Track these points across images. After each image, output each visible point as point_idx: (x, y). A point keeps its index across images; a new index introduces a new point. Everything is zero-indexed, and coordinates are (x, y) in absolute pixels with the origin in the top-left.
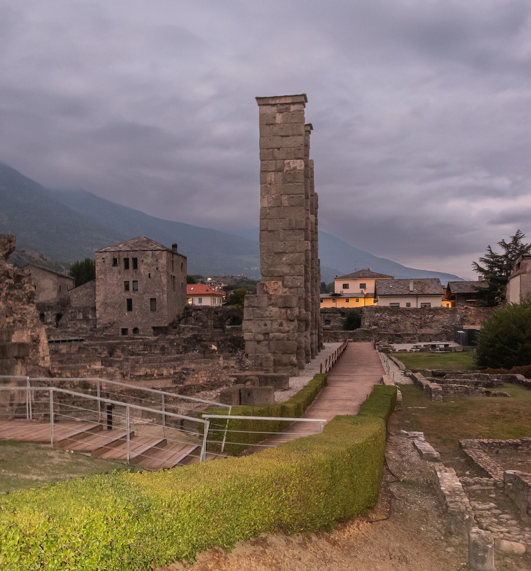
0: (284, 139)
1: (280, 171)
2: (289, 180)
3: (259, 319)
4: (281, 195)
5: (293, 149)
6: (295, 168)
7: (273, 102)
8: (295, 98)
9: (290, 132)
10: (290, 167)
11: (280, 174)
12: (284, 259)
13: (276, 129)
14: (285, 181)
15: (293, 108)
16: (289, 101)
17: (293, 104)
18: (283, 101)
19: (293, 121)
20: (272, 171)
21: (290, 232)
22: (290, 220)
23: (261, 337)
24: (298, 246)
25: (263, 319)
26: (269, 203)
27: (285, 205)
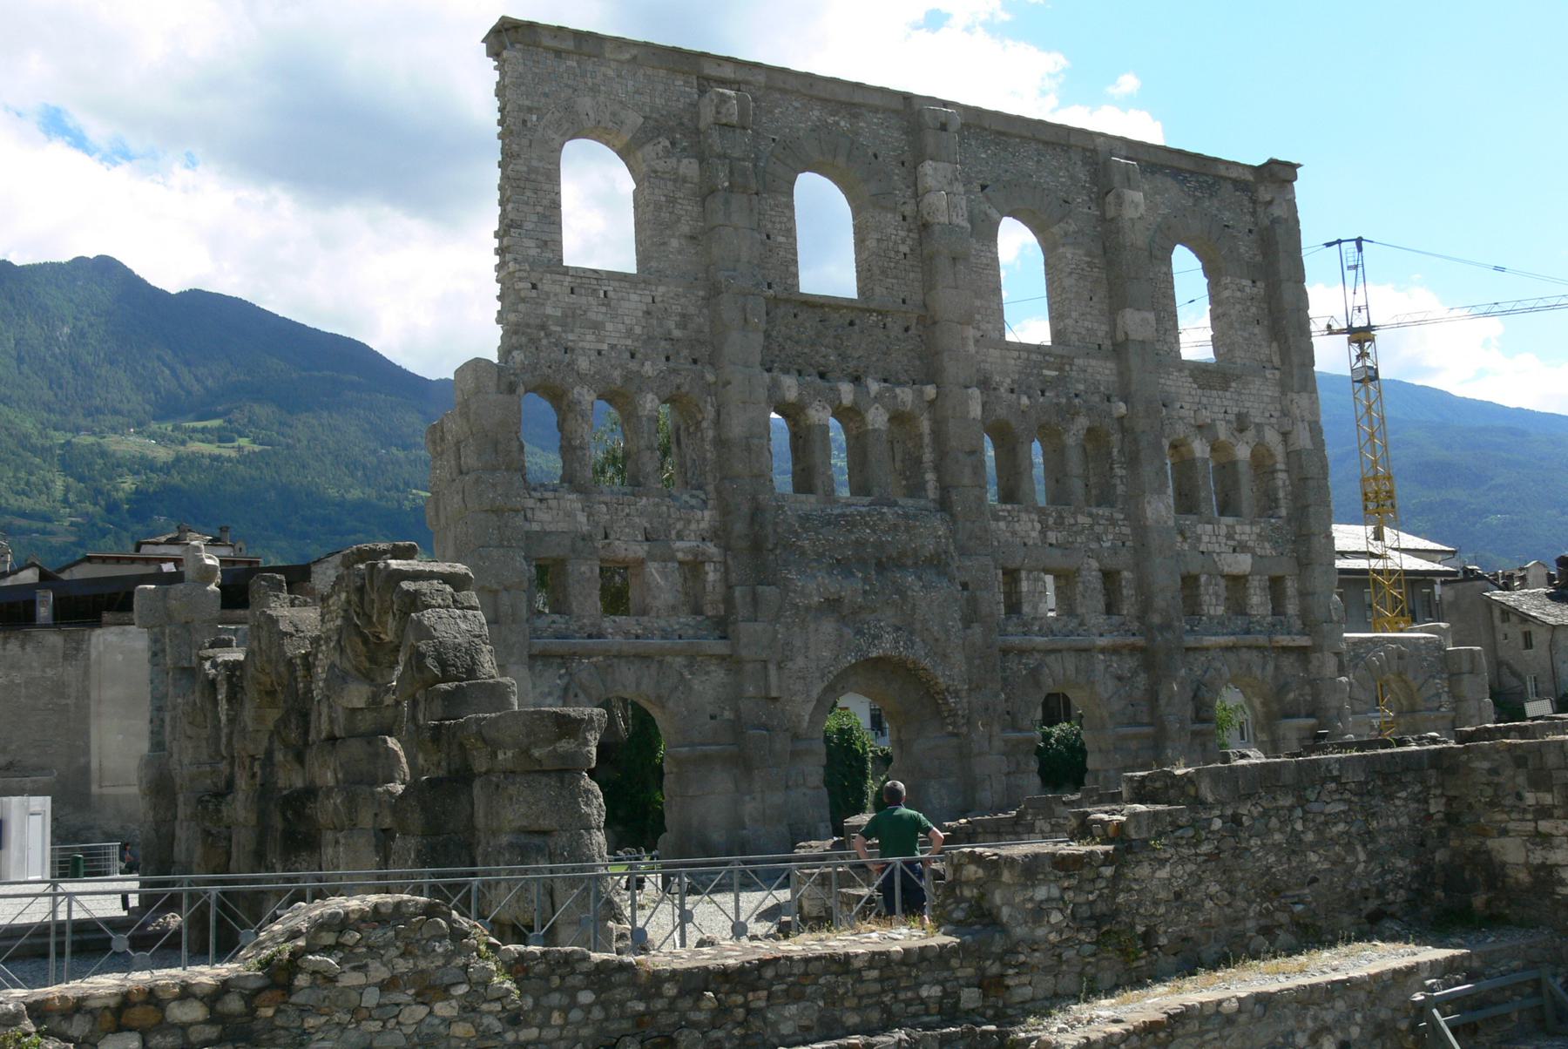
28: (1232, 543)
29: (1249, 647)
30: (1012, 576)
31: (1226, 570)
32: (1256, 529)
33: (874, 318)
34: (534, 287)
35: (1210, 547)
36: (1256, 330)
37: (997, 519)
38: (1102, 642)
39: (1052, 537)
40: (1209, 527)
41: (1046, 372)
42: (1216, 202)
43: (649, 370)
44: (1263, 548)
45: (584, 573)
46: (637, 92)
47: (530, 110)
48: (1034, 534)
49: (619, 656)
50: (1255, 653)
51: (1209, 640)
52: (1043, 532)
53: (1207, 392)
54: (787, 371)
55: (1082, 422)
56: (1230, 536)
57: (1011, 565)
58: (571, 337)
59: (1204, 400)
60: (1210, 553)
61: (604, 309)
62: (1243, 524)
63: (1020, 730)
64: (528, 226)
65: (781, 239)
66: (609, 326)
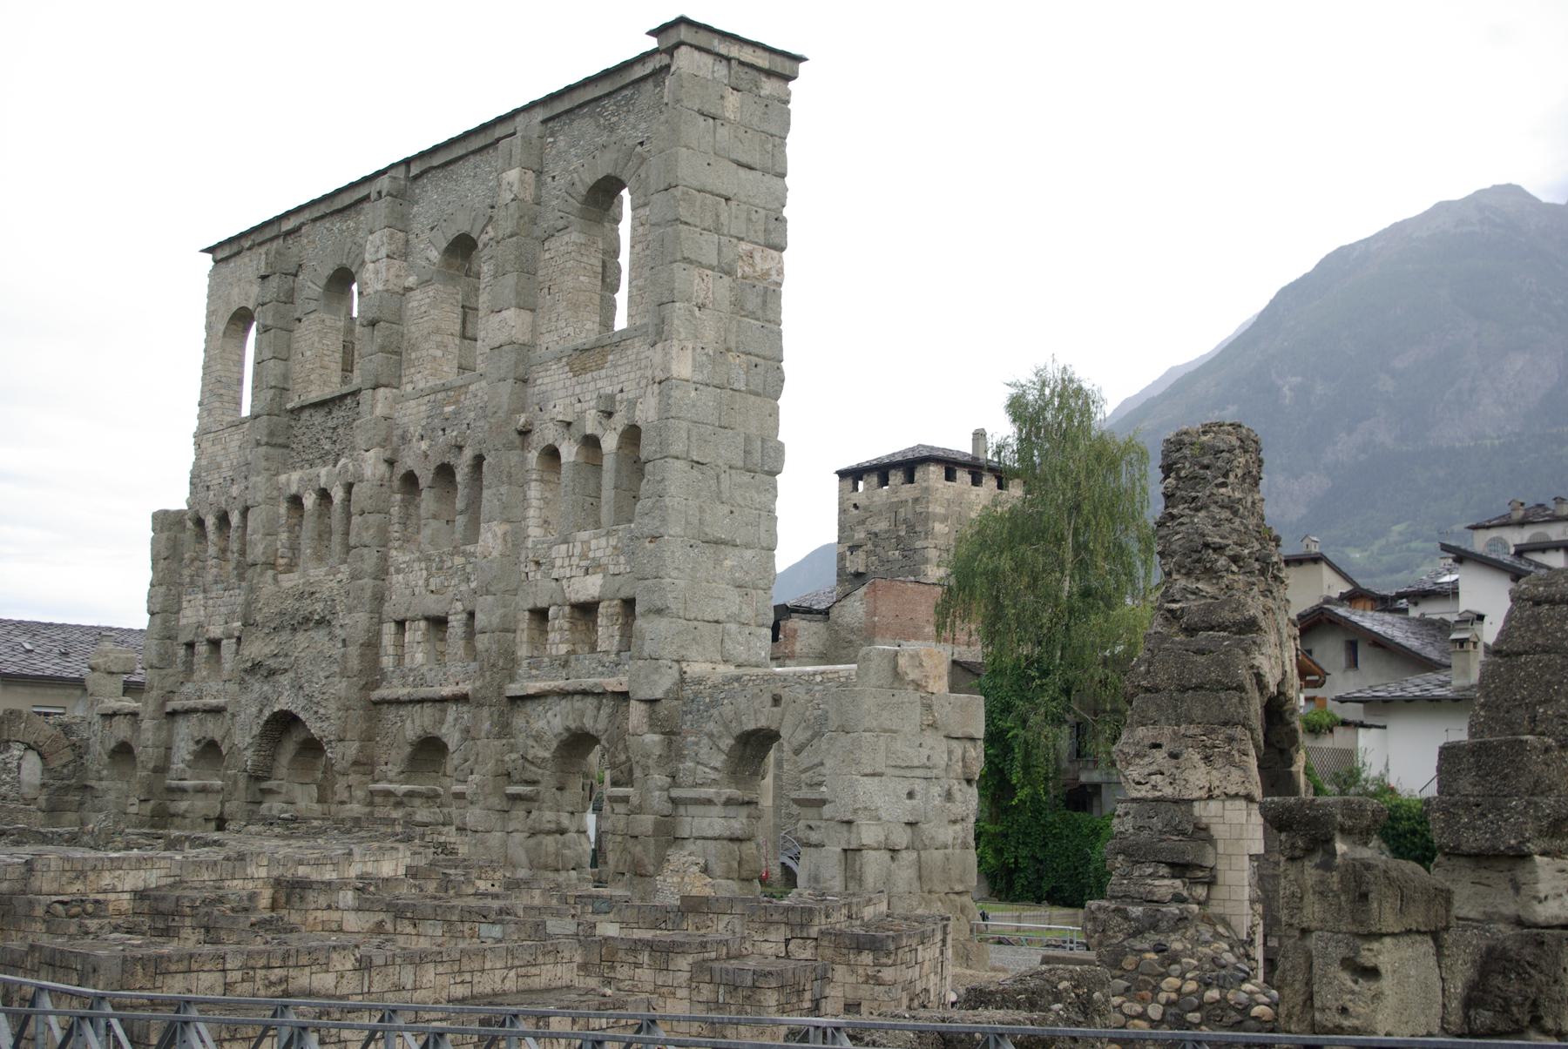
0: (742, 172)
1: (728, 274)
2: (750, 306)
3: (902, 772)
4: (729, 350)
5: (762, 212)
6: (766, 274)
7: (723, 49)
8: (778, 59)
9: (754, 158)
10: (752, 265)
11: (726, 278)
12: (728, 563)
13: (723, 132)
14: (738, 305)
15: (769, 87)
16: (763, 61)
17: (769, 73)
18: (747, 55)
19: (765, 127)
20: (712, 268)
21: (747, 477)
22: (748, 439)
23: (901, 837)
24: (763, 528)
25: (908, 773)
26: (698, 367)
27: (736, 386)
28: (583, 563)
29: (585, 693)
30: (401, 624)
31: (574, 598)
32: (613, 541)
33: (348, 400)
37: (398, 571)
38: (446, 691)
39: (434, 583)
42: (632, 118)
43: (235, 491)
44: (618, 564)
45: (202, 649)
48: (421, 582)
49: (205, 711)
50: (590, 702)
51: (533, 687)
52: (427, 580)
53: (582, 378)
54: (302, 467)
55: (468, 454)
56: (583, 556)
57: (400, 618)
59: (578, 389)
62: (597, 537)
63: (391, 782)
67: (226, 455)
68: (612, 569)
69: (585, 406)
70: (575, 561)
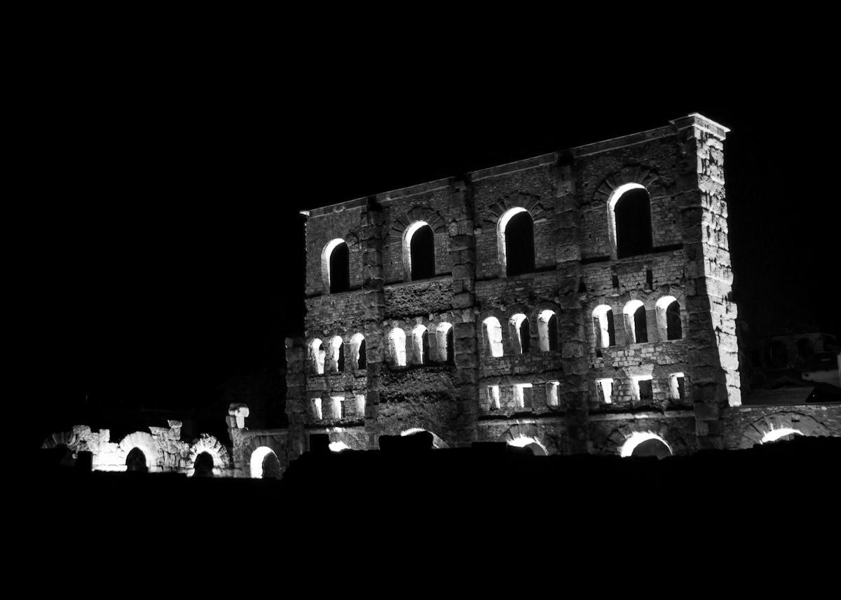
34: (311, 306)
35: (621, 364)
36: (672, 228)
39: (517, 370)
40: (621, 353)
41: (517, 289)
44: (664, 360)
46: (347, 221)
47: (312, 242)
52: (512, 369)
58: (322, 321)
60: (621, 367)
61: (332, 309)
64: (312, 285)
65: (396, 262)
66: (334, 315)
67: (335, 309)
68: (660, 362)
69: (628, 289)
70: (630, 359)
